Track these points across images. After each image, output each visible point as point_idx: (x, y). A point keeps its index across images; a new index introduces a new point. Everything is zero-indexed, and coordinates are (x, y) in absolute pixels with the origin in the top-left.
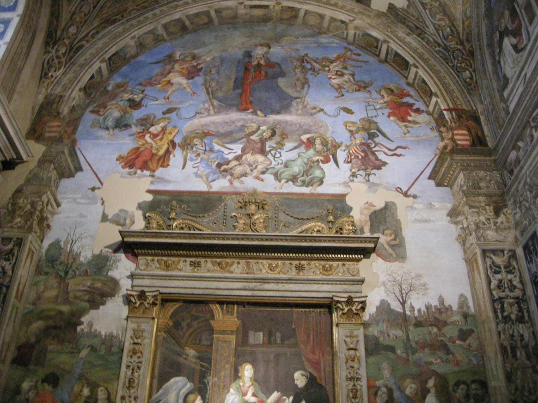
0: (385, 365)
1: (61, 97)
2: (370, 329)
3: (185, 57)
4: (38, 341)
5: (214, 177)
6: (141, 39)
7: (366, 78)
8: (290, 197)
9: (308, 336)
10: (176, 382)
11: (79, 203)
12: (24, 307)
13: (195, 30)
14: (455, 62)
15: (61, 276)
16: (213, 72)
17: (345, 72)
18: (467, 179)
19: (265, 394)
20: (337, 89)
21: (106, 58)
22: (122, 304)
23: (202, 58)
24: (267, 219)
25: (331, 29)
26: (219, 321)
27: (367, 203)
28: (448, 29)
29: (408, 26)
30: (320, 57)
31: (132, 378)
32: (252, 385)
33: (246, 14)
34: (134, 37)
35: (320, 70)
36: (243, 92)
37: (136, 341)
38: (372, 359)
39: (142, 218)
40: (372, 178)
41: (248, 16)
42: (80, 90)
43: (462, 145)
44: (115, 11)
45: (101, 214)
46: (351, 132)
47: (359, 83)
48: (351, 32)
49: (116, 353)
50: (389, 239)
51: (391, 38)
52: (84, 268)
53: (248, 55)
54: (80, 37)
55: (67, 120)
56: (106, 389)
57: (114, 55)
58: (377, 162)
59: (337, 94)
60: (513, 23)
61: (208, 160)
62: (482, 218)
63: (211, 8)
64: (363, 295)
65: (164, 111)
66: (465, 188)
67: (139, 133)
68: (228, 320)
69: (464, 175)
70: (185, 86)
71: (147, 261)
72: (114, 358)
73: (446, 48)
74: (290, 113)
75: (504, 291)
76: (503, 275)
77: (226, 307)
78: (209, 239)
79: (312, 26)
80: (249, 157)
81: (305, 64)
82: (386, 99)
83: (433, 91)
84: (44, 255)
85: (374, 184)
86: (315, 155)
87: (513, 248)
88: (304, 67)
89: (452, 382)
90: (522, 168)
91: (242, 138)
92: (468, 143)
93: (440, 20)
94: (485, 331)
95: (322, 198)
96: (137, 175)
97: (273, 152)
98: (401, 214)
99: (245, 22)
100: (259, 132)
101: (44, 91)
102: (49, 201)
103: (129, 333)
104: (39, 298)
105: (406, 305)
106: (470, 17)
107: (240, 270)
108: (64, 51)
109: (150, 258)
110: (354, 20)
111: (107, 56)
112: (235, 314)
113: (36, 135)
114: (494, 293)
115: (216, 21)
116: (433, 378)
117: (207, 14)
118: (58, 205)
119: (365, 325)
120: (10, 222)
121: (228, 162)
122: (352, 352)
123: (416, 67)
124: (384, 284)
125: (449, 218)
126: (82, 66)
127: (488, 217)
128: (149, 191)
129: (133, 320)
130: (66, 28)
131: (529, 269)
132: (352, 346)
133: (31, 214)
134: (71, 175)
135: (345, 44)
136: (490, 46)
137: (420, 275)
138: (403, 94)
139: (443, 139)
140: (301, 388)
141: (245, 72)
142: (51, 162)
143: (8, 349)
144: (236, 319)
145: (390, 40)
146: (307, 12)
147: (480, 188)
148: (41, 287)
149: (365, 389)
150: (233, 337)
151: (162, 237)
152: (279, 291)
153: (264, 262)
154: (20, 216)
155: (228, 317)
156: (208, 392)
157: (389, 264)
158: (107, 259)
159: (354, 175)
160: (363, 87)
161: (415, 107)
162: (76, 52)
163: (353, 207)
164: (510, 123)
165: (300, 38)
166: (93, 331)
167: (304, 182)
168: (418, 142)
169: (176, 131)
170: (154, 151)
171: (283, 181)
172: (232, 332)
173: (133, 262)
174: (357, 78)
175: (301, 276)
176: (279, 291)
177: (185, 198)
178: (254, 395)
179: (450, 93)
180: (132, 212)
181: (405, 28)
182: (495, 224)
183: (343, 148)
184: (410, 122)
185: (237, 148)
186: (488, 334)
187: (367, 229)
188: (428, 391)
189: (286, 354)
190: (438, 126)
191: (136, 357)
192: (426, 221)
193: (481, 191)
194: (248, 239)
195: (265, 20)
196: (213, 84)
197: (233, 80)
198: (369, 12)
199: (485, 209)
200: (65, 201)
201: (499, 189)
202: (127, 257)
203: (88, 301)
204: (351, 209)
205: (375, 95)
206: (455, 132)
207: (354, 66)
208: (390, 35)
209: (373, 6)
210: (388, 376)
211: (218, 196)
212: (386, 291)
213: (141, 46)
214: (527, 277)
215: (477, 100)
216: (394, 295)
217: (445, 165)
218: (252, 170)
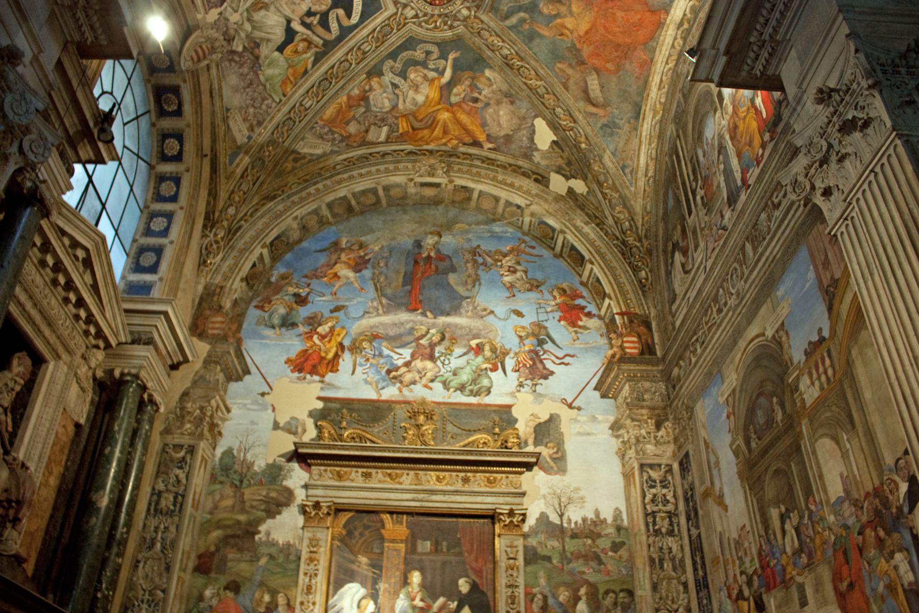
0: (541, 574)
1: (222, 288)
2: (530, 540)
3: (352, 245)
4: (218, 550)
5: (384, 384)
6: (304, 221)
7: (539, 276)
8: (458, 407)
9: (472, 546)
11: (249, 409)
12: (202, 516)
13: (362, 213)
14: (632, 259)
15: (236, 486)
16: (382, 265)
17: (518, 267)
18: (632, 390)
20: (508, 288)
21: (268, 243)
22: (297, 513)
23: (371, 246)
24: (435, 430)
25: (506, 215)
28: (627, 223)
29: (587, 214)
30: (493, 249)
33: (416, 194)
34: (296, 218)
35: (492, 265)
36: (412, 288)
37: (312, 549)
38: (529, 569)
39: (313, 426)
40: (538, 388)
41: (418, 197)
42: (242, 280)
43: (630, 354)
44: (276, 186)
46: (520, 337)
47: (532, 282)
48: (527, 219)
50: (551, 451)
51: (568, 228)
52: (259, 477)
53: (418, 244)
54: (239, 217)
55: (230, 316)
56: (286, 595)
57: (277, 238)
58: (545, 372)
59: (508, 294)
60: (683, 241)
61: (377, 365)
62: (643, 432)
63: (378, 184)
64: (524, 507)
65: (332, 307)
66: (629, 400)
67: (307, 333)
69: (630, 386)
70: (352, 280)
72: (293, 566)
73: (624, 243)
74: (460, 315)
76: (658, 490)
78: (380, 451)
79: (485, 211)
80: (418, 364)
81: (477, 258)
82: (558, 301)
83: (607, 291)
85: (540, 395)
86: (484, 363)
87: (669, 462)
88: (475, 261)
89: (602, 590)
90: (681, 387)
91: (412, 342)
92: (636, 351)
93: (619, 212)
95: (489, 408)
97: (442, 358)
98: (564, 428)
99: (414, 204)
100: (429, 336)
101: (203, 281)
102: (218, 407)
103: (306, 542)
104: (216, 507)
106: (650, 212)
108: (222, 234)
109: (322, 468)
110: (530, 205)
111: (268, 240)
113: (198, 331)
114: (648, 507)
115: (384, 202)
117: (374, 191)
118: (228, 411)
119: (525, 536)
120: (180, 428)
121: (397, 369)
122: (512, 561)
123: (592, 263)
124: (544, 497)
126: (242, 251)
128: (319, 398)
129: (310, 529)
130: (225, 209)
131: (683, 485)
132: (512, 556)
133: (201, 420)
134: (239, 379)
135: (520, 235)
136: (665, 251)
138: (576, 296)
139: (612, 347)
141: (414, 266)
142: (217, 363)
143: (188, 558)
145: (567, 231)
146: (481, 193)
147: (644, 400)
149: (522, 596)
150: (403, 545)
151: (334, 449)
153: (433, 473)
154: (190, 422)
155: (397, 527)
157: (550, 477)
158: (280, 468)
159: (521, 385)
160: (535, 286)
161: (586, 311)
162: (234, 234)
163: (520, 419)
164: (675, 339)
165: (473, 226)
167: (471, 391)
168: (586, 350)
169: (344, 332)
170: (323, 354)
171: (452, 390)
172: (402, 541)
173: (307, 471)
174: (530, 275)
175: (467, 488)
177: (356, 406)
178: (422, 600)
179: (624, 294)
181: (584, 215)
182: (655, 437)
183: (512, 355)
184: (580, 327)
185: (407, 353)
186: (638, 546)
187: (531, 441)
188: (579, 599)
190: (608, 332)
192: (589, 434)
193: (645, 403)
194: (417, 452)
195: (436, 202)
196: (382, 279)
197: (402, 274)
198: (547, 194)
199: (647, 423)
200: (235, 407)
201: (663, 401)
202: (301, 467)
203: (266, 511)
204: (516, 421)
205: (547, 295)
206: (625, 339)
207: (527, 262)
208: (567, 224)
209: (551, 187)
210: (544, 584)
211: (387, 405)
213: (304, 228)
215: (650, 305)
217: (612, 376)
218: (421, 378)
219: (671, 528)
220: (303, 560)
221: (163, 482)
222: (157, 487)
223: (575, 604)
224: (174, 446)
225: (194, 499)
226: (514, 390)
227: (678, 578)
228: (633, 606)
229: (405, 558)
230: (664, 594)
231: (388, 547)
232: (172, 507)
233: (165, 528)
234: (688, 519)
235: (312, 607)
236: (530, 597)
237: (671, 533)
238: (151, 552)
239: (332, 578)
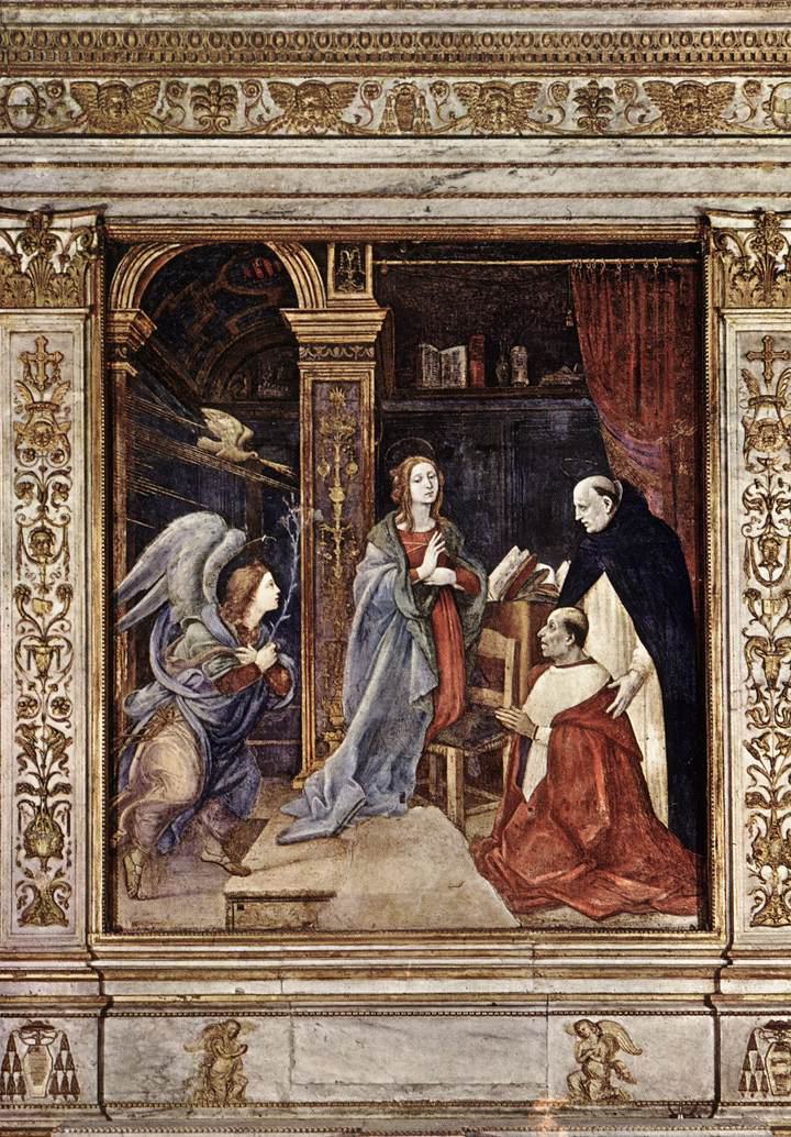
31: (43, 529)
32: (438, 527)
37: (37, 398)
71: (36, 91)
112: (369, 281)
140: (594, 533)
152: (517, 195)
176: (517, 195)
178: (443, 561)
235: (58, 607)
239: (119, 499)
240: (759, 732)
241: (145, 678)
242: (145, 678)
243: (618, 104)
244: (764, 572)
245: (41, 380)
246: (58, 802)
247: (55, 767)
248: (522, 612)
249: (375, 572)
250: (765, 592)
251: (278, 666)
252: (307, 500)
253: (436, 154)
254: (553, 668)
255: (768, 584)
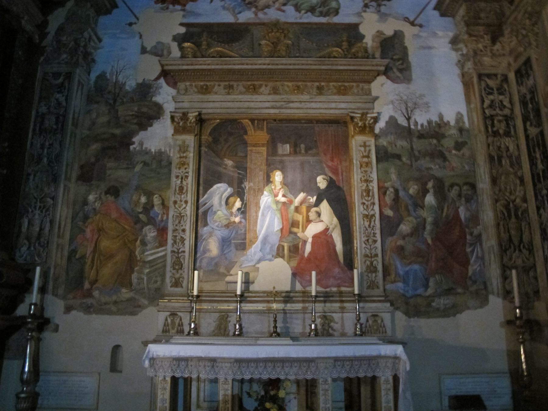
0: (392, 170)
10: (218, 188)
15: (110, 104)
19: (293, 195)
26: (252, 136)
27: (378, 32)
32: (282, 187)
37: (182, 155)
40: (383, 9)
45: (140, 47)
49: (166, 166)
56: (160, 196)
62: (480, 46)
68: (259, 135)
75: (495, 110)
76: (496, 97)
77: (257, 123)
84: (93, 86)
89: (447, 184)
94: (477, 143)
96: (169, 10)
98: (409, 42)
104: (94, 123)
105: (411, 121)
107: (268, 92)
112: (265, 128)
114: (487, 111)
116: (432, 181)
118: (100, 40)
122: (365, 160)
124: (392, 102)
125: (450, 45)
127: (485, 45)
131: (519, 92)
132: (364, 154)
134: (108, 12)
137: (424, 96)
144: (266, 134)
147: (480, 18)
148: (94, 115)
150: (265, 148)
152: (302, 108)
156: (246, 195)
157: (396, 85)
166: (144, 149)
171: (303, 12)
172: (263, 145)
176: (302, 108)
178: (284, 196)
180: (168, 44)
182: (491, 51)
187: (378, 55)
188: (427, 191)
189: (309, 162)
191: (184, 168)
193: (481, 21)
204: (363, 37)
210: (395, 179)
212: (394, 108)
214: (516, 99)
216: (400, 112)
219: (507, 130)
220: (173, 165)
221: (45, 105)
222: (40, 110)
223: (424, 196)
224: (52, 73)
225: (73, 118)
226: (360, 10)
227: (515, 174)
228: (475, 198)
229: (267, 160)
230: (503, 187)
231: (251, 150)
232: (55, 127)
233: (50, 145)
234: (525, 119)
235: (184, 206)
236: (383, 190)
237: (507, 134)
238: (40, 166)
240: (367, 238)
241: (206, 224)
242: (206, 224)
243: (326, 88)
244: (366, 198)
245: (183, 150)
246: (181, 256)
247: (181, 246)
248: (304, 209)
249: (266, 199)
250: (366, 203)
251: (240, 222)
252: (249, 180)
253: (282, 99)
254: (312, 223)
255: (368, 201)
